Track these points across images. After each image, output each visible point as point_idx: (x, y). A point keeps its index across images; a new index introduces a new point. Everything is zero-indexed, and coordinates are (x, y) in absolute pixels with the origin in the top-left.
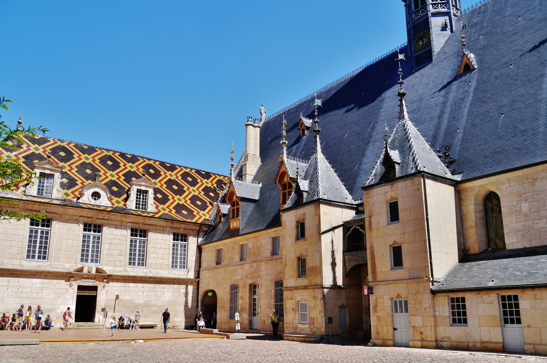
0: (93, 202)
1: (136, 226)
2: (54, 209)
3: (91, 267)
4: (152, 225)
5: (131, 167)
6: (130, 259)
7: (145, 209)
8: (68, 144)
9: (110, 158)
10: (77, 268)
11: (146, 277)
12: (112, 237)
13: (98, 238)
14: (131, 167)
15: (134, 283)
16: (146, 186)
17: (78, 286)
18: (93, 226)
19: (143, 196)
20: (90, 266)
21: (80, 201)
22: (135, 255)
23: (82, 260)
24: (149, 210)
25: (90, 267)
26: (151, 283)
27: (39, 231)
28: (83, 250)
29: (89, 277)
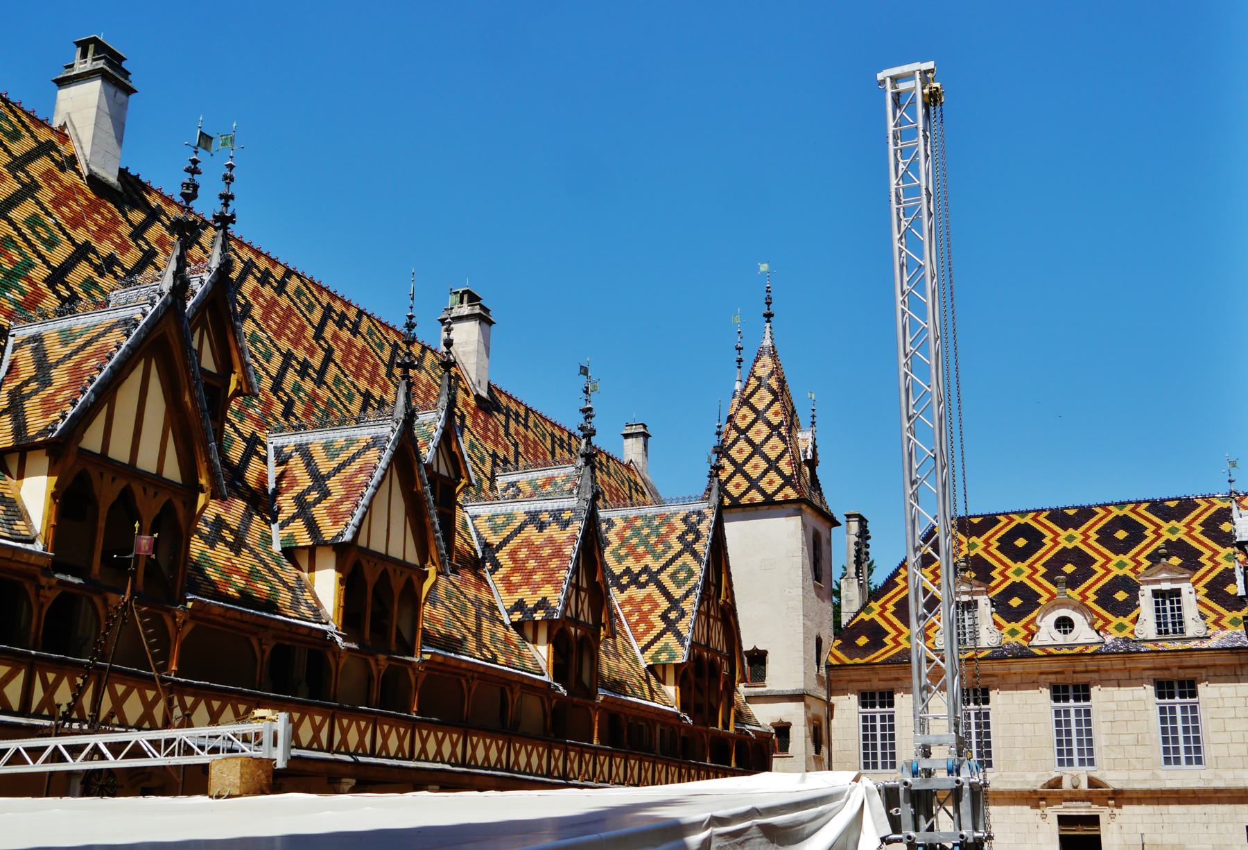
0: (1060, 639)
1: (1166, 675)
2: (987, 667)
3: (1077, 777)
4: (1204, 667)
5: (1174, 531)
6: (1166, 750)
7: (1182, 631)
8: (1034, 519)
9: (1123, 522)
10: (1046, 779)
11: (1205, 791)
12: (1113, 706)
13: (1088, 712)
14: (1174, 531)
15: (1179, 803)
16: (1172, 580)
17: (1059, 817)
18: (1071, 690)
19: (1172, 602)
20: (1075, 773)
21: (1035, 642)
22: (1175, 740)
23: (1061, 763)
24: (1189, 634)
25: (1076, 776)
26: (1223, 803)
27: (972, 714)
28: (1059, 742)
29: (1075, 797)
